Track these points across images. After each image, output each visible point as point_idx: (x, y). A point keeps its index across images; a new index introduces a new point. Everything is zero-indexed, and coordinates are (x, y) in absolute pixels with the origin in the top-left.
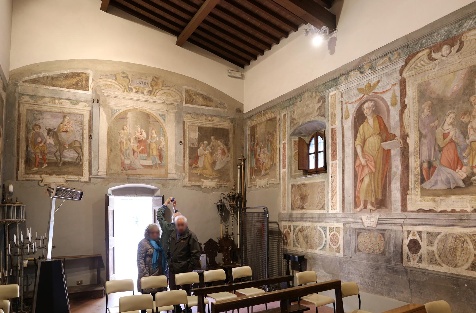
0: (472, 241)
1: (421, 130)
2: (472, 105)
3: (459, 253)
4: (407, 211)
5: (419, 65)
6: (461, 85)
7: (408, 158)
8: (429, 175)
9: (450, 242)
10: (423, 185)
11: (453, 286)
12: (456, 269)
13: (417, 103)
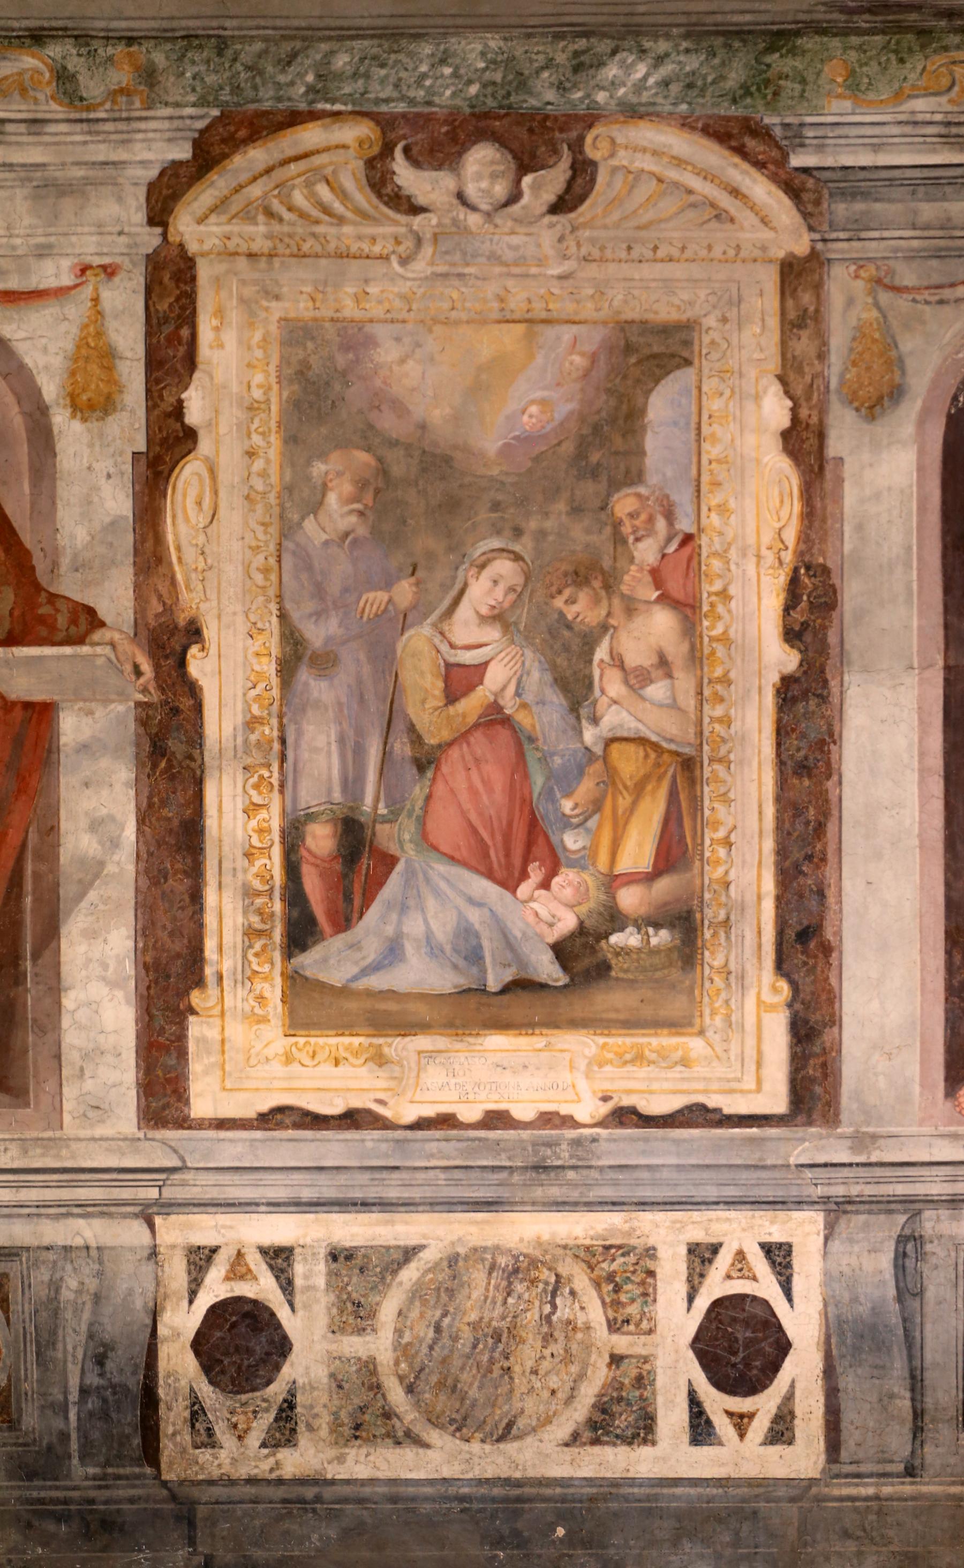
0: (597, 1284)
1: (295, 615)
2: (619, 539)
3: (527, 1354)
4: (184, 1123)
5: (299, 198)
6: (564, 409)
7: (199, 783)
8: (348, 898)
9: (478, 1298)
10: (308, 961)
11: (487, 1551)
12: (509, 1447)
13: (273, 438)
